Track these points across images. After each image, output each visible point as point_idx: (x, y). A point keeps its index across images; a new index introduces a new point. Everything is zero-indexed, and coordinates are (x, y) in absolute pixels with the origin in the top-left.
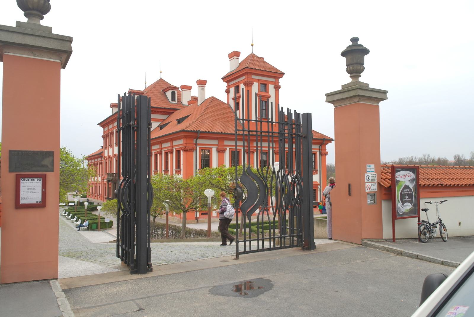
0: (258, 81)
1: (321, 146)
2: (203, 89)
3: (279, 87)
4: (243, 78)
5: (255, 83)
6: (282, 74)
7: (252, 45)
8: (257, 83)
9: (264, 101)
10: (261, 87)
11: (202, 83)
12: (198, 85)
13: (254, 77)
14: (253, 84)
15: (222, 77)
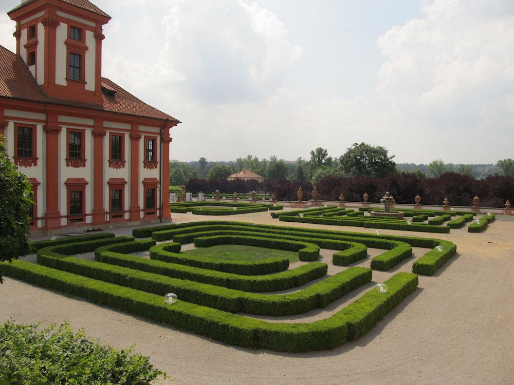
1: (162, 130)
5: (61, 23)
6: (106, 19)
8: (66, 25)
9: (77, 55)
10: (72, 32)
13: (60, 13)
15: (8, 11)
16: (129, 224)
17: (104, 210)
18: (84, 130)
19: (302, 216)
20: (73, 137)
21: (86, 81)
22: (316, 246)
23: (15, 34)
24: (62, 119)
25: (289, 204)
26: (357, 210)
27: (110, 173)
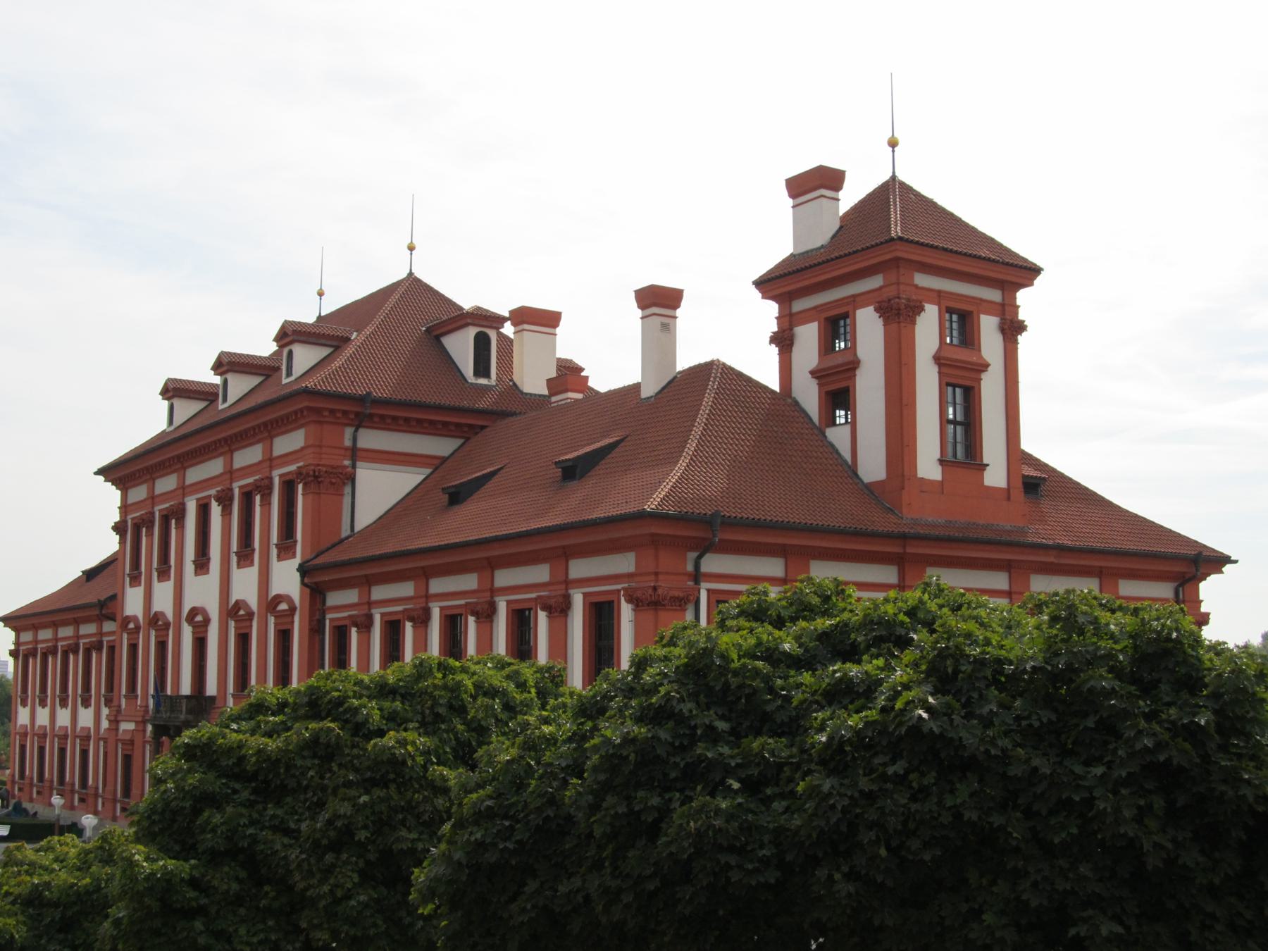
0: (938, 297)
3: (1020, 327)
5: (928, 307)
14: (922, 309)
21: (985, 462)
23: (775, 339)
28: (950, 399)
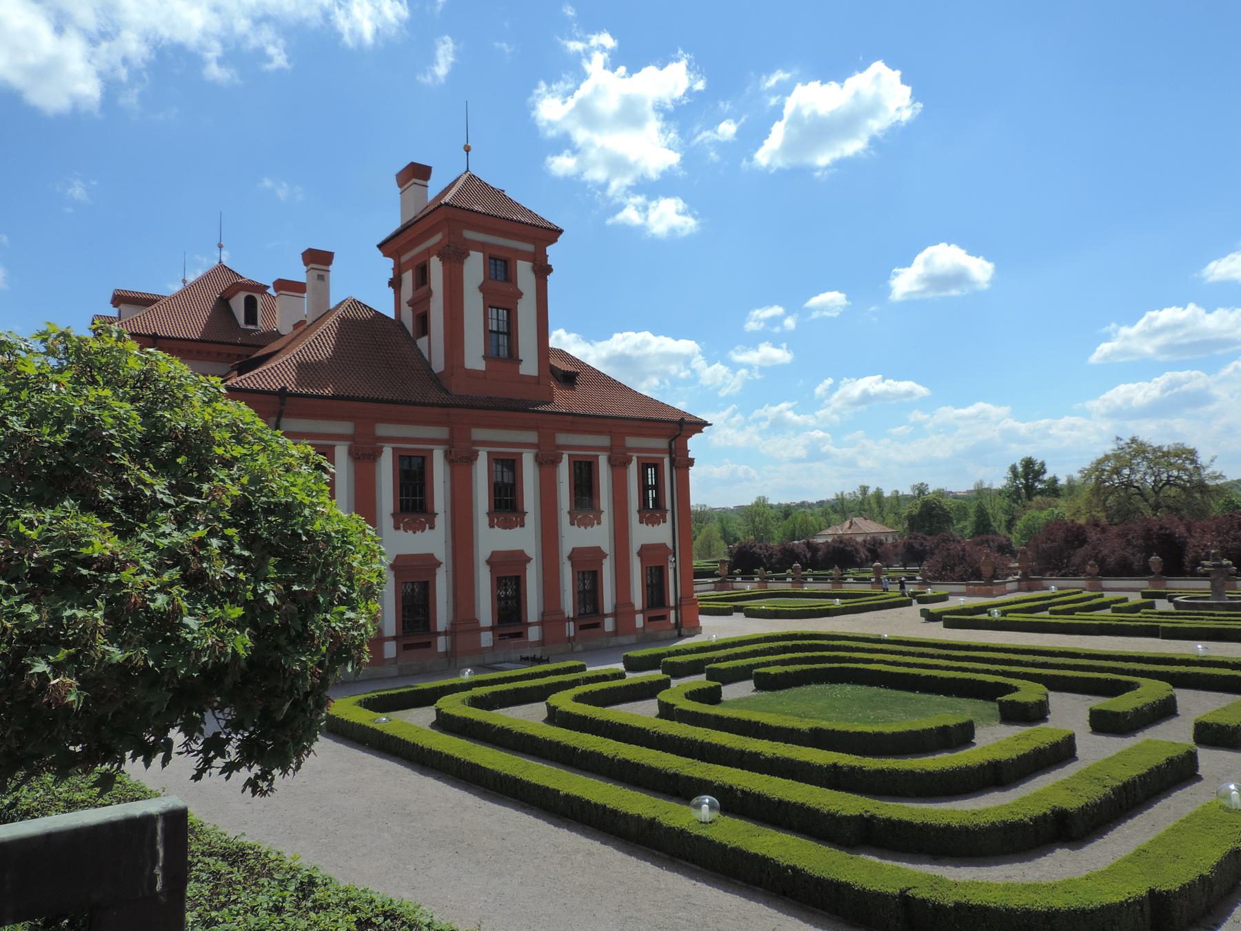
0: (481, 247)
2: (321, 278)
3: (549, 270)
4: (437, 238)
6: (554, 233)
7: (467, 149)
8: (481, 255)
11: (318, 259)
12: (306, 264)
13: (469, 235)
15: (379, 242)
16: (614, 641)
17: (563, 613)
18: (521, 454)
19: (996, 614)
20: (499, 467)
22: (1041, 688)
23: (391, 283)
24: (478, 434)
25: (962, 588)
26: (1135, 598)
27: (573, 537)
28: (495, 316)
